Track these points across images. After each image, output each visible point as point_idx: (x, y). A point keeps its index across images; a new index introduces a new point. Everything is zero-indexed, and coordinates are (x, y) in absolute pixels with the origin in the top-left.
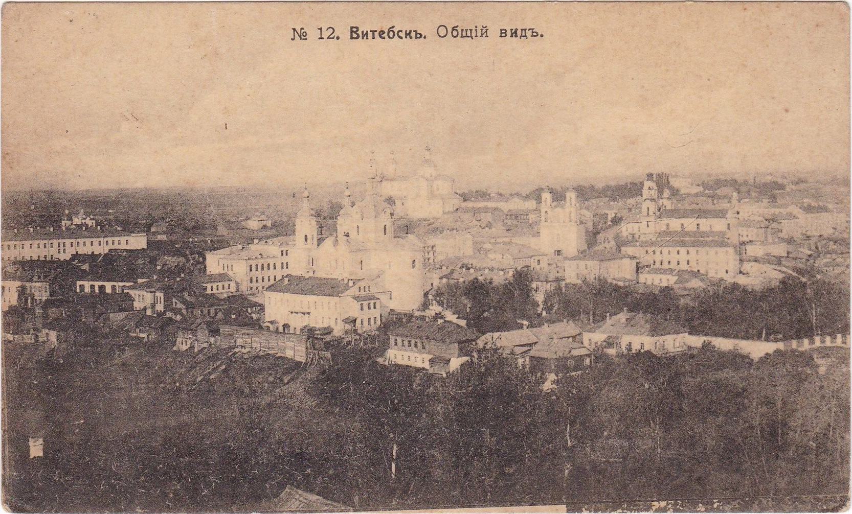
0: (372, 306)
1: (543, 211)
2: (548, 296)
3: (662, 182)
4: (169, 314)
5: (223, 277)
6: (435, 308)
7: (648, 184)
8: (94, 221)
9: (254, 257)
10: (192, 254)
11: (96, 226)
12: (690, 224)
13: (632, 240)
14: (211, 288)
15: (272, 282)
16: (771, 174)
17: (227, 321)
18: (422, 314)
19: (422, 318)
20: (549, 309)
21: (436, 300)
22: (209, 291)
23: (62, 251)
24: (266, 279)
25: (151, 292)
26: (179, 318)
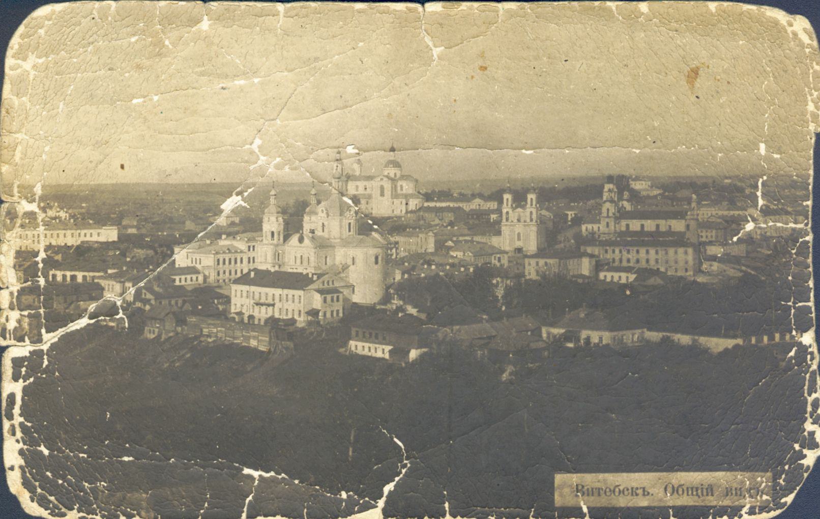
0: (335, 299)
1: (504, 211)
2: (508, 291)
3: (621, 182)
4: (138, 304)
5: (192, 270)
6: (396, 302)
7: (607, 187)
8: (68, 215)
9: (221, 252)
10: (161, 246)
11: (70, 219)
12: (650, 225)
13: (592, 240)
14: (179, 281)
15: (239, 275)
16: (730, 178)
17: (195, 313)
18: (383, 307)
19: (385, 311)
20: (508, 304)
21: (398, 294)
22: (177, 283)
23: (36, 241)
24: (233, 273)
25: (120, 282)
26: (148, 307)
